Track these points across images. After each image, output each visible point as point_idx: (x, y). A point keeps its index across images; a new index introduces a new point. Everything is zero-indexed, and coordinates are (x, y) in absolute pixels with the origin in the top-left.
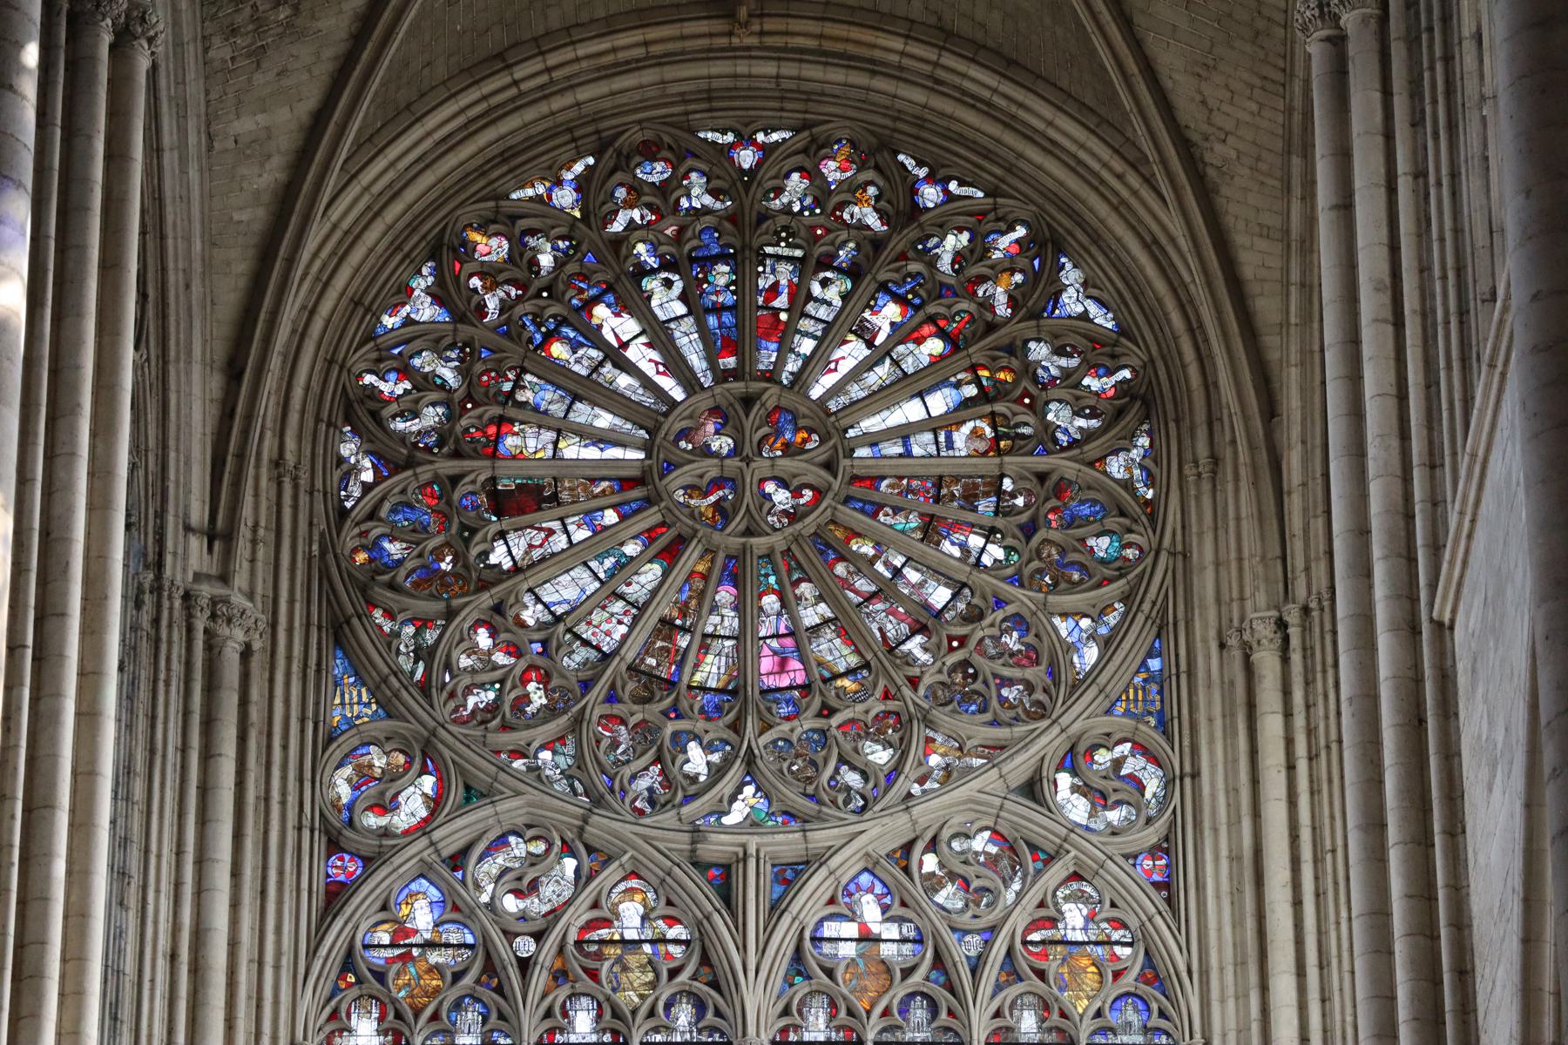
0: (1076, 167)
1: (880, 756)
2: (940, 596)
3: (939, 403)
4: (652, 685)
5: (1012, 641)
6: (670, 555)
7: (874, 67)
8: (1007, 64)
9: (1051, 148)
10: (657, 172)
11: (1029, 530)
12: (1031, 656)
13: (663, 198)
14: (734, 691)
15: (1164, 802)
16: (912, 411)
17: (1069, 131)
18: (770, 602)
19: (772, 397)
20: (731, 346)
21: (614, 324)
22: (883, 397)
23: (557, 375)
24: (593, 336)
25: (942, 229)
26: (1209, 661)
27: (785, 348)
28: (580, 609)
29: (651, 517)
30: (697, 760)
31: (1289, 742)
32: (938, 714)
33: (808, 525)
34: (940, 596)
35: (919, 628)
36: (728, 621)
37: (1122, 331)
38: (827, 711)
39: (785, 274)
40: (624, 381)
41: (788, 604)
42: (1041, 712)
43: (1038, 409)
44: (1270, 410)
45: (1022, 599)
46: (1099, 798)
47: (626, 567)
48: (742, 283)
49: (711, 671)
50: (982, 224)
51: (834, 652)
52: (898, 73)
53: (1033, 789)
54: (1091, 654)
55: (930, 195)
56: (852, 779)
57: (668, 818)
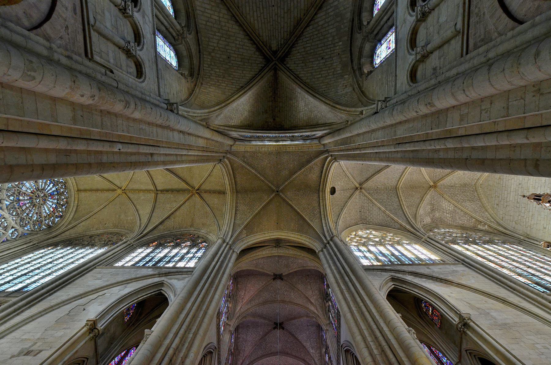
0: (69, 218)
1: (14, 214)
2: (30, 215)
3: (47, 211)
4: (19, 193)
5: (27, 222)
6: (32, 193)
7: (74, 202)
8: (76, 211)
9: (70, 215)
10: (63, 187)
11: (38, 221)
12: (26, 224)
13: (62, 188)
14: (19, 200)
15: (12, 239)
16: (47, 209)
17: (71, 216)
18: (28, 202)
19: (46, 199)
20: (50, 195)
21: (51, 185)
22: (47, 207)
23: (46, 182)
24: (50, 184)
25: (62, 209)
26: (28, 239)
27: (51, 199)
28: (26, 186)
29: (35, 191)
30: (12, 198)
31: (24, 248)
32: (19, 218)
33: (36, 203)
34: (30, 215)
35: (27, 214)
36: (26, 198)
37: (55, 224)
38: (18, 208)
39: (57, 198)
40: (47, 187)
41: (28, 203)
42: (20, 226)
43: (48, 219)
44: (53, 237)
45: (31, 222)
46: (12, 233)
47: (30, 189)
48: (56, 195)
49: (21, 198)
50: (62, 212)
51: (24, 208)
52: (74, 203)
53: (13, 227)
54: (26, 229)
55: (64, 207)
56: (11, 212)
57: (6, 196)
